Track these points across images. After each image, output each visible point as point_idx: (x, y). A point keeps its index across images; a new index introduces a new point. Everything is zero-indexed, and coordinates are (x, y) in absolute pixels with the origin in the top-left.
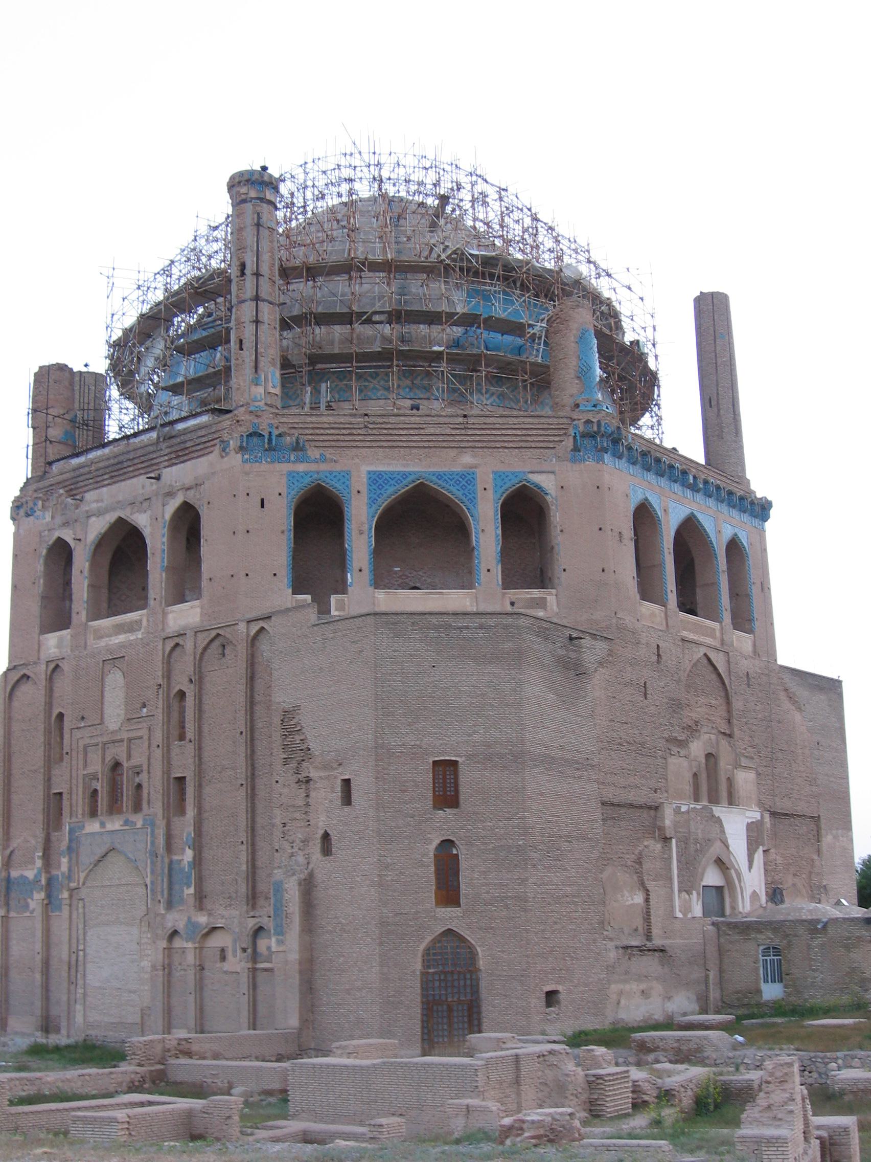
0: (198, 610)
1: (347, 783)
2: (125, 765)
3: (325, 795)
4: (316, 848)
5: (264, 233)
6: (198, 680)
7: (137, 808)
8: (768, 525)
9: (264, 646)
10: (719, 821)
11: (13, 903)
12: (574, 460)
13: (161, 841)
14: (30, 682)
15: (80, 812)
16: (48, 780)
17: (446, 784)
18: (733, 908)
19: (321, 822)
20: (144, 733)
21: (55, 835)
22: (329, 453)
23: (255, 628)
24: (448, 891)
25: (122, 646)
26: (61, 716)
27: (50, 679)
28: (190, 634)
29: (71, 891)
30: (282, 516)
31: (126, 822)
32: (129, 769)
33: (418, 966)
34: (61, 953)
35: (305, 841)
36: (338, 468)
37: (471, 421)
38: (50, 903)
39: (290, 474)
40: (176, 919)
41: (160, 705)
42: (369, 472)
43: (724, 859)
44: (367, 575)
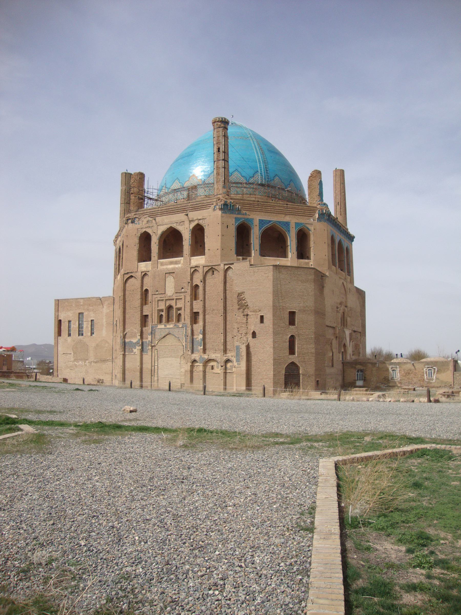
0: (204, 259)
1: (262, 317)
2: (175, 307)
3: (254, 320)
4: (250, 336)
6: (204, 281)
7: (178, 320)
8: (353, 243)
9: (230, 273)
10: (345, 333)
11: (127, 350)
13: (189, 332)
14: (133, 278)
15: (156, 321)
16: (142, 311)
18: (346, 358)
19: (252, 328)
20: (183, 297)
21: (144, 329)
22: (247, 212)
23: (226, 267)
24: (292, 351)
25: (174, 269)
26: (147, 290)
27: (143, 278)
28: (201, 267)
29: (152, 347)
31: (175, 326)
32: (176, 308)
33: (284, 372)
34: (147, 366)
35: (246, 333)
36: (250, 217)
37: (289, 206)
38: (142, 350)
39: (236, 218)
40: (196, 356)
41: (189, 288)
42: (259, 220)
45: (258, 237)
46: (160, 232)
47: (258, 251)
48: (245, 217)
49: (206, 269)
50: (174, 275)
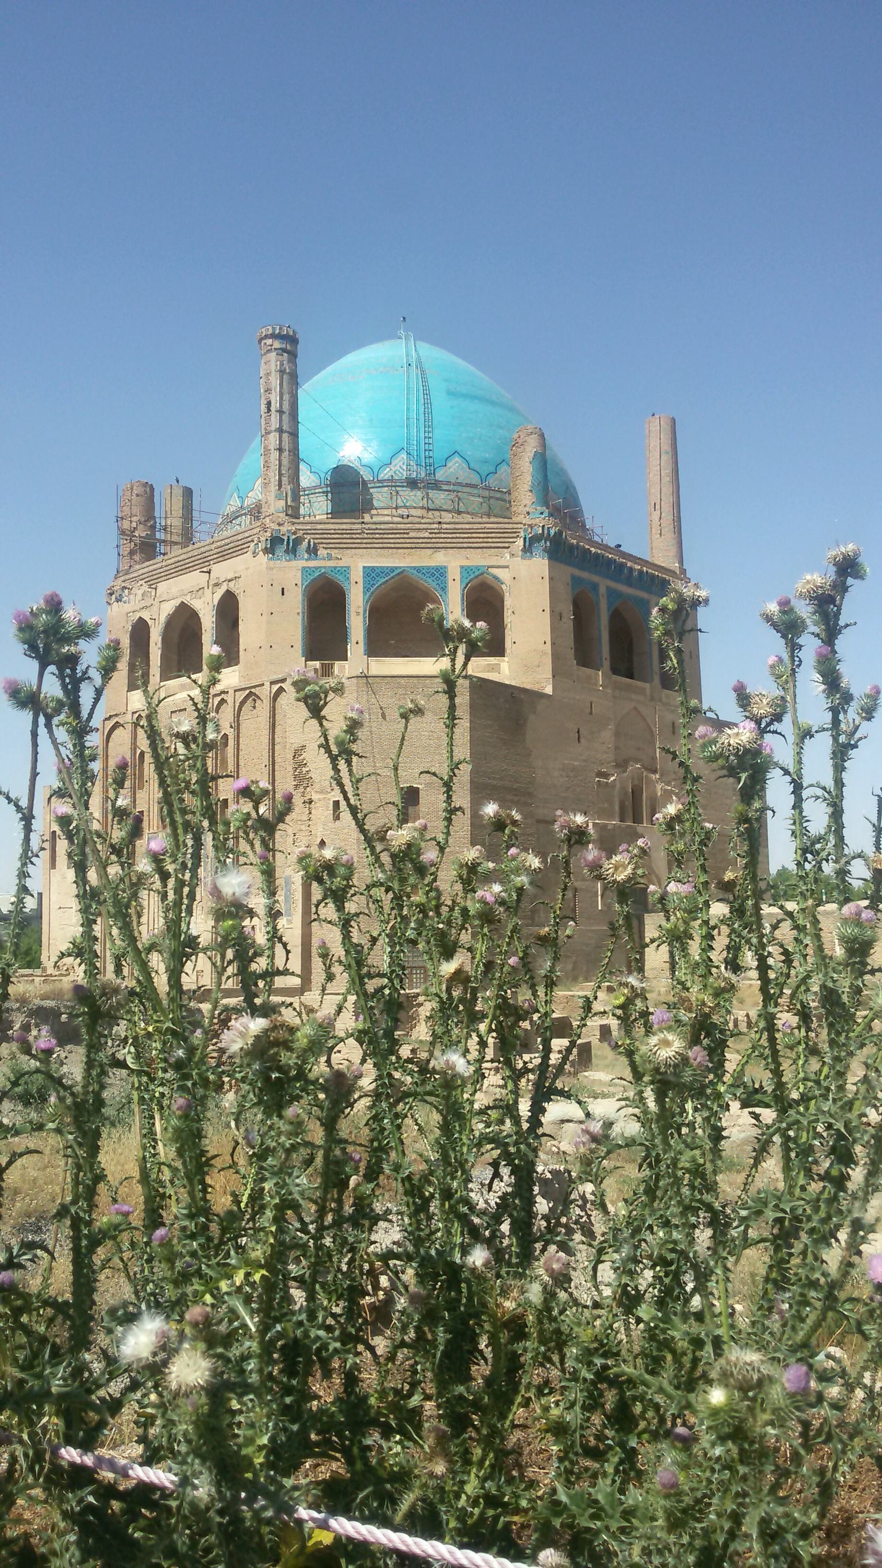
6: (237, 726)
22: (334, 552)
23: (275, 687)
28: (231, 692)
30: (296, 602)
36: (341, 563)
39: (304, 568)
44: (361, 647)
45: (361, 610)
46: (163, 618)
49: (241, 696)
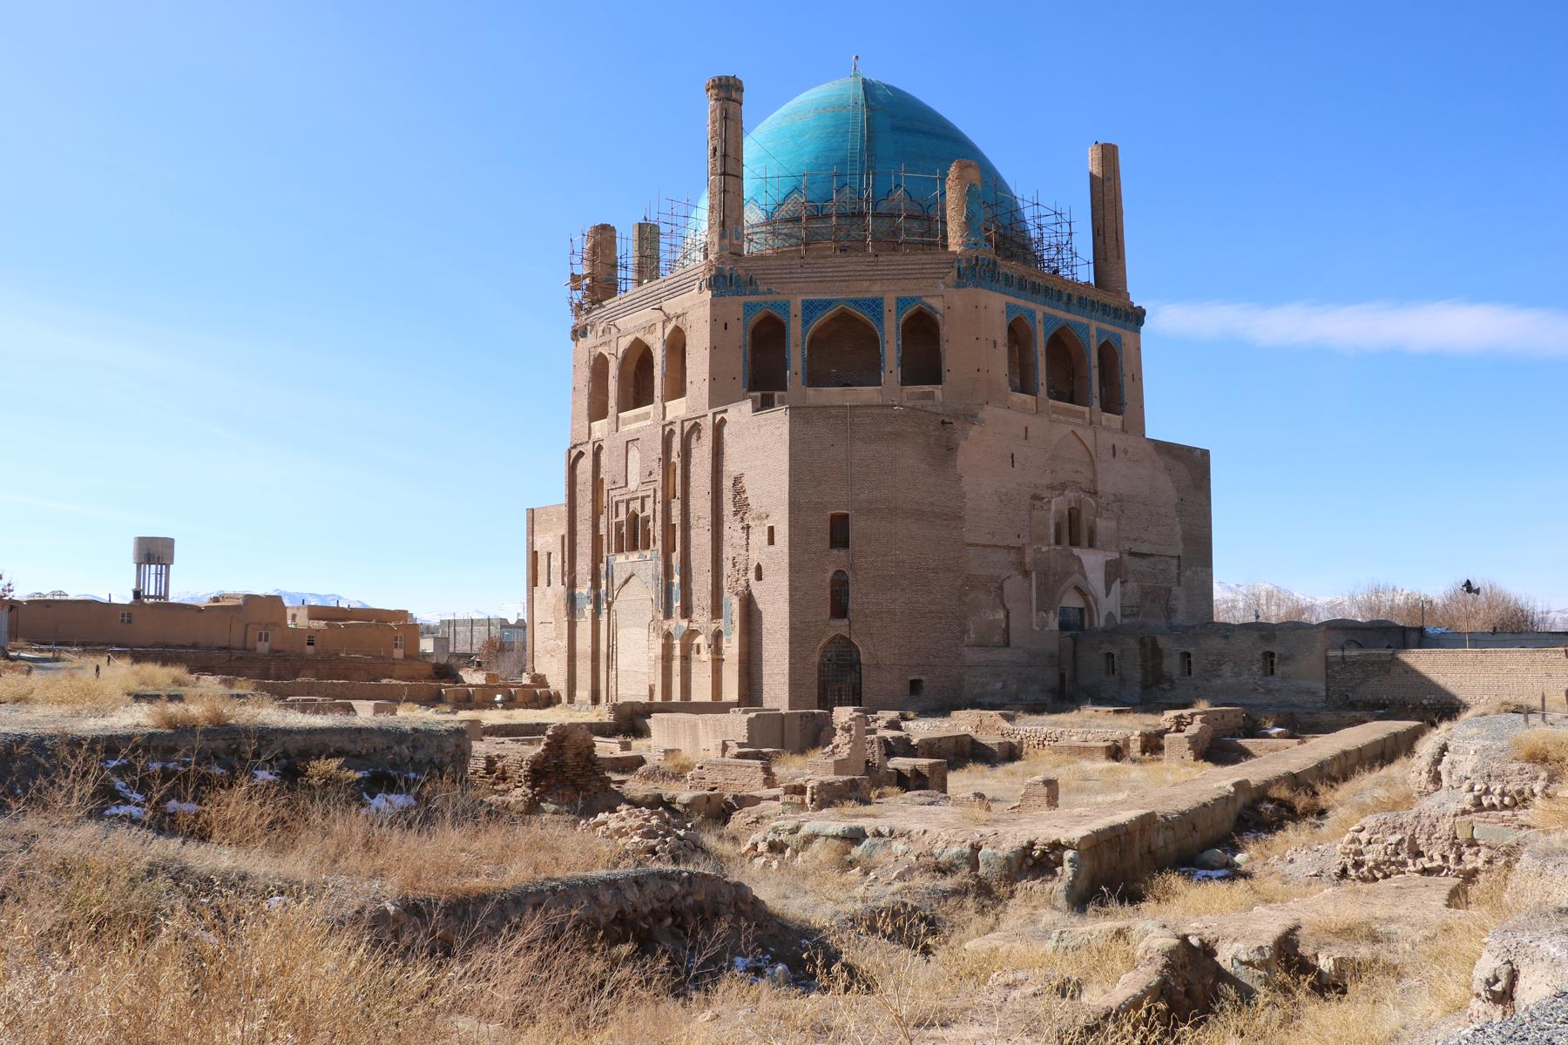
1: (771, 529)
3: (759, 536)
4: (752, 575)
5: (731, 124)
7: (647, 547)
12: (958, 286)
17: (839, 532)
18: (1091, 624)
20: (651, 493)
24: (840, 609)
33: (817, 660)
36: (780, 298)
39: (745, 305)
43: (1082, 586)
44: (799, 379)
47: (800, 374)
48: (770, 298)
49: (687, 426)
50: (638, 443)
